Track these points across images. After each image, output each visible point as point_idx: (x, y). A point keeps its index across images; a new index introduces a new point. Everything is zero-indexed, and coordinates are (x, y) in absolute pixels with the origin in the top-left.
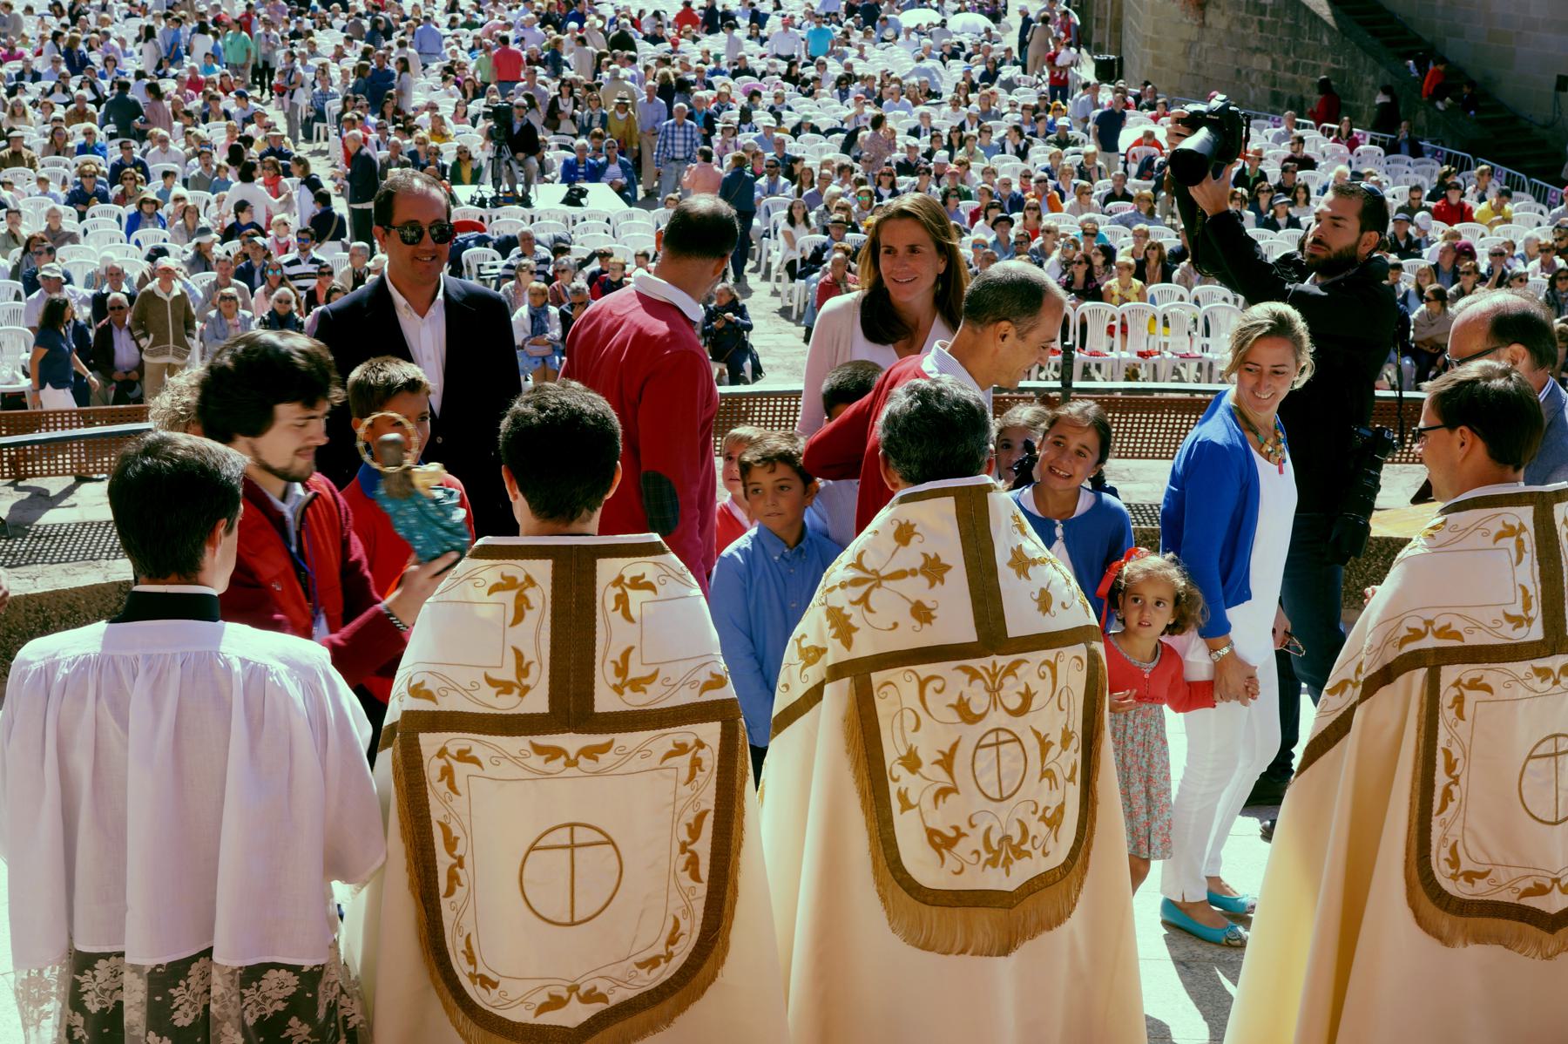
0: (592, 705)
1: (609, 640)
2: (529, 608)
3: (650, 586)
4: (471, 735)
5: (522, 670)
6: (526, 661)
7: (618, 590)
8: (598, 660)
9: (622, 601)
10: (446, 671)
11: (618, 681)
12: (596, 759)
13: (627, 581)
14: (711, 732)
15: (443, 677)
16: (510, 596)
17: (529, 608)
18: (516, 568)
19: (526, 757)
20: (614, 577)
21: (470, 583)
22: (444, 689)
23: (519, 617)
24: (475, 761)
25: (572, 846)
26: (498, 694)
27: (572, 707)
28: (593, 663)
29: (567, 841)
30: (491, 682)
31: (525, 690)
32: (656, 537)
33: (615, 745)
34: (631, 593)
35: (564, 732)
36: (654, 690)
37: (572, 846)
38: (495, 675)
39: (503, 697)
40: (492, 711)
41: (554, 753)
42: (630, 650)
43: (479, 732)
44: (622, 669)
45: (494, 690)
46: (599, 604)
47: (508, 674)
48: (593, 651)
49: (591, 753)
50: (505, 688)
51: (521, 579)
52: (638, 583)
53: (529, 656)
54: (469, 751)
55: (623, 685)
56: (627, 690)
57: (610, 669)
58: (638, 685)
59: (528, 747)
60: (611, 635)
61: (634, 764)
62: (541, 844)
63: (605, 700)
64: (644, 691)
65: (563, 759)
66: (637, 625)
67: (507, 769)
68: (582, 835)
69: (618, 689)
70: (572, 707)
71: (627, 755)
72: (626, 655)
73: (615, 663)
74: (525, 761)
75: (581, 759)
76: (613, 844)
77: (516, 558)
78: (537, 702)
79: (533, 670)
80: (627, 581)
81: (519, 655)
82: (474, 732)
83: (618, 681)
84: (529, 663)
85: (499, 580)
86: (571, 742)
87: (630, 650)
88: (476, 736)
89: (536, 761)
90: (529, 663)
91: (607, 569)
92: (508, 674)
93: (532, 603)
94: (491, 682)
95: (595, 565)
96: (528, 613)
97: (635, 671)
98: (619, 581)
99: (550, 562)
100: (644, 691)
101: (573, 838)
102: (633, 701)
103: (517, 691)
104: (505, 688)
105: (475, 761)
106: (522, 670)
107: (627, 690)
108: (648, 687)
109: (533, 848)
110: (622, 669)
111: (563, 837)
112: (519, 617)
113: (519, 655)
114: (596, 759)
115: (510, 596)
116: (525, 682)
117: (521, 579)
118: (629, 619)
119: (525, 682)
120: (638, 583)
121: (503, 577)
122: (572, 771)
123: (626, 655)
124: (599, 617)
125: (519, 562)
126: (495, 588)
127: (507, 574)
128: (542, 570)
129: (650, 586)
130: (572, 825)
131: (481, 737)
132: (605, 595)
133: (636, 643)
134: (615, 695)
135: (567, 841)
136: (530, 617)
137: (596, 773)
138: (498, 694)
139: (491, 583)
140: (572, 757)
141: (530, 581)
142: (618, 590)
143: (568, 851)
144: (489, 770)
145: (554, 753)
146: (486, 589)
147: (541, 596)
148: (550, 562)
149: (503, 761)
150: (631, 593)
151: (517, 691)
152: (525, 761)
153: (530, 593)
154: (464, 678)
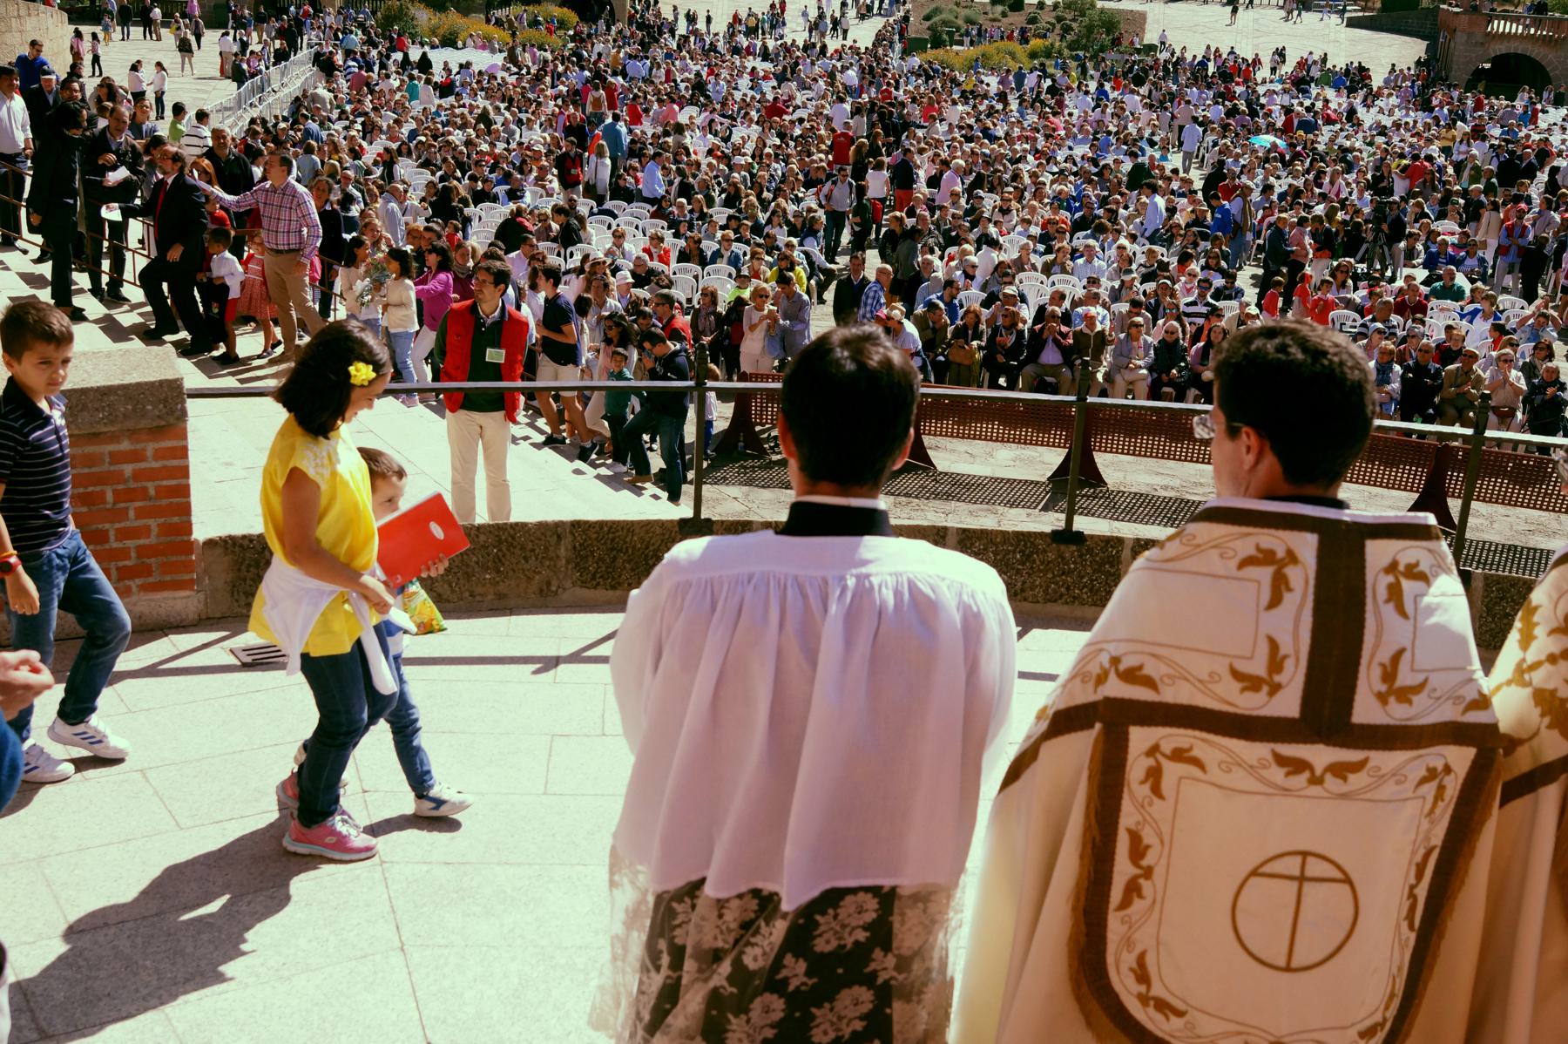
0: (1350, 714)
2: (1289, 589)
4: (1197, 733)
5: (1276, 662)
6: (1282, 652)
7: (1391, 579)
9: (1395, 593)
10: (1177, 656)
11: (1383, 688)
12: (1345, 779)
13: (1401, 568)
14: (1460, 758)
15: (1171, 663)
16: (1265, 574)
17: (1289, 589)
18: (1276, 540)
19: (1264, 767)
20: (1386, 561)
21: (1214, 553)
22: (1169, 676)
24: (1197, 762)
25: (1302, 879)
26: (1244, 690)
27: (1326, 714)
28: (1357, 664)
29: (1297, 872)
30: (1237, 675)
31: (1275, 689)
33: (1370, 764)
34: (1407, 585)
35: (1313, 742)
36: (1419, 700)
37: (1302, 879)
38: (1242, 667)
39: (1248, 694)
40: (1231, 709)
41: (1297, 766)
42: (1401, 652)
43: (1209, 730)
44: (1389, 674)
45: (1237, 686)
46: (1369, 593)
47: (1258, 667)
49: (1340, 770)
50: (1251, 683)
51: (1281, 553)
53: (1286, 647)
54: (1190, 749)
55: (1390, 692)
56: (1392, 700)
57: (1376, 672)
58: (1405, 695)
59: (1270, 757)
60: (1383, 630)
61: (1389, 789)
62: (1266, 869)
63: (1366, 710)
64: (1410, 702)
65: (1307, 774)
67: (1239, 779)
68: (1315, 868)
69: (1382, 698)
70: (1326, 714)
71: (1381, 779)
72: (1397, 657)
73: (1383, 666)
74: (1264, 773)
75: (1328, 777)
76: (1347, 880)
77: (1277, 528)
78: (1288, 704)
79: (1289, 665)
80: (1401, 568)
81: (1273, 645)
82: (1201, 729)
83: (1383, 688)
84: (1285, 657)
85: (1252, 551)
86: (1321, 755)
87: (1401, 652)
88: (1204, 735)
89: (1277, 774)
90: (1285, 657)
91: (1378, 552)
92: (1258, 667)
94: (1237, 675)
95: (1363, 547)
96: (1287, 596)
97: (1405, 678)
98: (1392, 568)
100: (1410, 702)
101: (1303, 870)
102: (1397, 714)
103: (1265, 689)
104: (1251, 683)
105: (1197, 762)
106: (1276, 662)
107: (1392, 700)
108: (1415, 699)
109: (1254, 873)
110: (1389, 674)
111: (1292, 866)
113: (1273, 645)
114: (1345, 779)
115: (1265, 574)
116: (1277, 678)
117: (1281, 553)
118: (1402, 613)
119: (1277, 678)
120: (1414, 573)
121: (1258, 548)
122: (1315, 790)
123: (1397, 657)
125: (1281, 533)
128: (1306, 545)
130: (1305, 854)
131: (1211, 737)
132: (1377, 582)
133: (1408, 644)
134: (1375, 704)
135: (1297, 872)
136: (1290, 601)
137: (1343, 796)
138: (1244, 690)
139: (1242, 555)
140: (1318, 772)
141: (1292, 558)
142: (1391, 579)
143: (1295, 885)
144: (1215, 773)
145: (1297, 766)
146: (1233, 564)
147: (1303, 576)
149: (1235, 769)
150: (1407, 585)
151: (1265, 689)
152: (1264, 773)
153: (1292, 573)
154: (1200, 666)
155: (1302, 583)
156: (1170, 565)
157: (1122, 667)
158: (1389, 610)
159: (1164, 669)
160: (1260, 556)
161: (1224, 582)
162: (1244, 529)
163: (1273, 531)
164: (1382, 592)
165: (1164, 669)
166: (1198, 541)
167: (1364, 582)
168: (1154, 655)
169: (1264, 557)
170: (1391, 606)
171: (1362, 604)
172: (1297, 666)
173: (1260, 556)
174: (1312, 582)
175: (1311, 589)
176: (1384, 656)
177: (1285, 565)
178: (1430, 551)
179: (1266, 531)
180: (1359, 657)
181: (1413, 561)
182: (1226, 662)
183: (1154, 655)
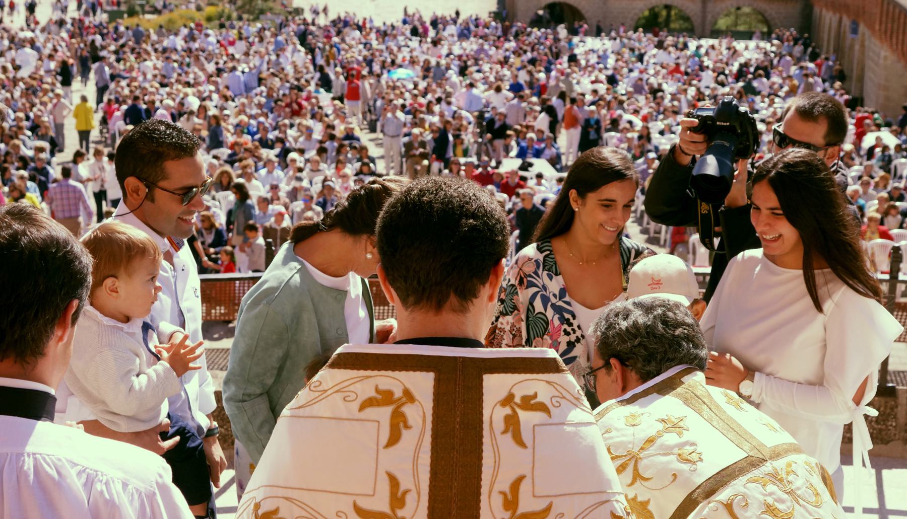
1: (497, 466)
2: (407, 427)
3: (542, 408)
6: (402, 488)
7: (508, 411)
8: (484, 490)
9: (512, 424)
13: (517, 400)
15: (302, 505)
16: (384, 413)
17: (407, 427)
18: (394, 381)
20: (503, 394)
21: (338, 397)
23: (394, 439)
28: (479, 494)
32: (552, 354)
34: (523, 415)
42: (520, 479)
44: (511, 503)
48: (479, 479)
51: (398, 393)
52: (529, 403)
53: (406, 483)
60: (500, 463)
66: (529, 451)
72: (516, 484)
79: (410, 499)
80: (517, 400)
81: (394, 482)
84: (406, 492)
85: (373, 394)
87: (520, 479)
90: (406, 492)
91: (494, 386)
93: (411, 422)
95: (481, 380)
96: (405, 433)
98: (508, 400)
99: (431, 375)
112: (394, 439)
113: (394, 482)
115: (384, 413)
117: (398, 393)
120: (529, 403)
121: (377, 391)
123: (516, 484)
124: (486, 440)
125: (397, 374)
126: (369, 403)
127: (382, 387)
128: (422, 384)
129: (542, 408)
132: (493, 413)
133: (525, 470)
136: (408, 438)
141: (409, 396)
142: (508, 411)
146: (356, 405)
147: (420, 414)
148: (431, 375)
150: (523, 415)
153: (409, 411)
155: (421, 423)
156: (301, 412)
157: (260, 512)
158: (506, 441)
159: (298, 512)
160: (379, 397)
161: (346, 422)
162: (362, 373)
163: (390, 373)
164: (499, 425)
165: (298, 512)
166: (324, 386)
167: (481, 415)
168: (287, 499)
169: (385, 398)
170: (509, 435)
171: (481, 436)
172: (419, 501)
173: (379, 397)
174: (429, 419)
175: (429, 426)
176: (504, 484)
177: (403, 404)
178: (548, 382)
179: (383, 373)
180: (479, 487)
181: (531, 393)
182: (350, 499)
183: (287, 499)
